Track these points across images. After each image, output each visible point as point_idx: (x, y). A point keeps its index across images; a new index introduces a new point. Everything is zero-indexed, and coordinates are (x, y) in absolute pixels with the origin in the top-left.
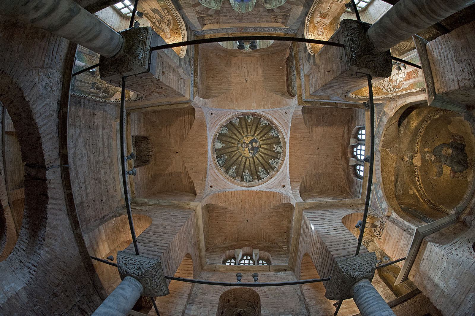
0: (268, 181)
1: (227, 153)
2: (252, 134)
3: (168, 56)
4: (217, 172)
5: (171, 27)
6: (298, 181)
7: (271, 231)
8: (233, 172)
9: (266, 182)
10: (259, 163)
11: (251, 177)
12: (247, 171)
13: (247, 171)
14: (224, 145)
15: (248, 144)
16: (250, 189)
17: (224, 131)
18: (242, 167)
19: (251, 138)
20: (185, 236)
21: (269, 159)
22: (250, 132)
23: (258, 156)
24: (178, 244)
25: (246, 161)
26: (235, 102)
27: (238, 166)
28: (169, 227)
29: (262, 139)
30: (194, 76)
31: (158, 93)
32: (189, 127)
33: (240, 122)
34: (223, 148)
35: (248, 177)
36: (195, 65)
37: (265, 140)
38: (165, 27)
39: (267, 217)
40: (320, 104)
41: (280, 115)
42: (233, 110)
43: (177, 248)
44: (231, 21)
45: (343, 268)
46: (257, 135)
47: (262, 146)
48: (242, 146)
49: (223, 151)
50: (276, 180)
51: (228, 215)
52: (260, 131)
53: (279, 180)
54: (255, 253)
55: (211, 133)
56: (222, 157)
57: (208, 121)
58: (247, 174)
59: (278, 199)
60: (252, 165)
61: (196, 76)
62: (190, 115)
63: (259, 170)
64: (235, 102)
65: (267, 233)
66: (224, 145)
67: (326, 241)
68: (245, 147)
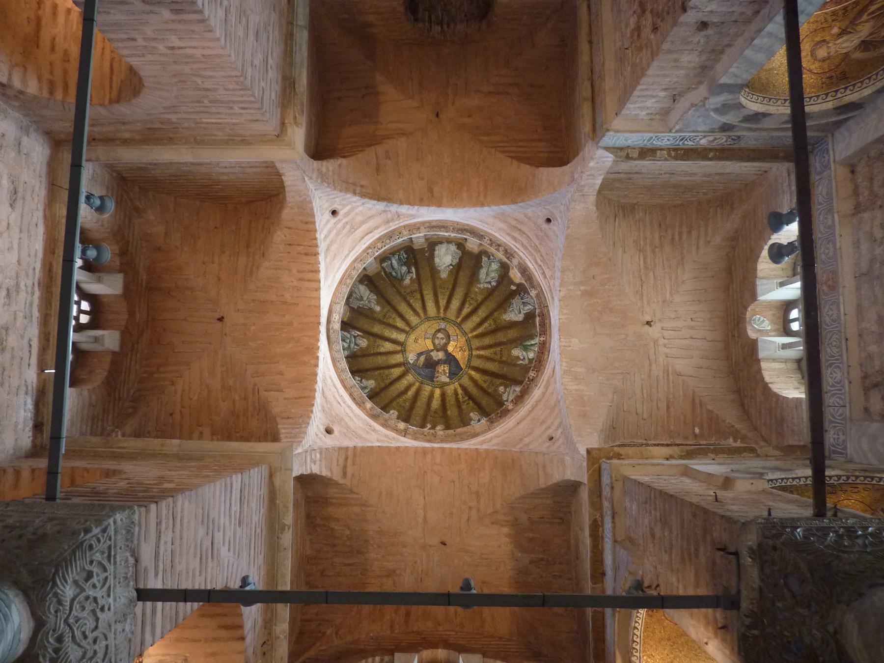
0: (345, 387)
1: (420, 284)
2: (476, 363)
3: (753, 39)
4: (376, 235)
5: (858, 55)
6: (345, 474)
7: (179, 394)
8: (361, 299)
9: (342, 382)
10: (387, 382)
12: (363, 343)
13: (363, 343)
14: (444, 275)
15: (444, 349)
16: (323, 329)
17: (487, 274)
18: (377, 329)
20: (208, 85)
21: (398, 411)
23: (410, 378)
24: (189, 51)
26: (582, 288)
27: (380, 316)
28: (241, 33)
29: (460, 391)
30: (674, 150)
31: (638, 29)
32: (511, 152)
33: (513, 325)
34: (434, 271)
36: (711, 150)
37: (457, 399)
38: (861, 34)
39: (231, 382)
40: (595, 521)
41: (544, 422)
42: (558, 282)
43: (177, 43)
44: (865, 247)
45: (104, 531)
47: (438, 392)
48: (439, 331)
49: (426, 272)
50: (348, 411)
51: (242, 260)
52: (485, 385)
53: (347, 419)
54: (110, 339)
55: (490, 220)
57: (529, 212)
58: (356, 344)
59: (293, 411)
60: (380, 360)
61: (673, 153)
62: (546, 155)
63: (367, 379)
64: (582, 288)
65: (173, 384)
66: (444, 275)
67: (187, 502)
68: (437, 342)
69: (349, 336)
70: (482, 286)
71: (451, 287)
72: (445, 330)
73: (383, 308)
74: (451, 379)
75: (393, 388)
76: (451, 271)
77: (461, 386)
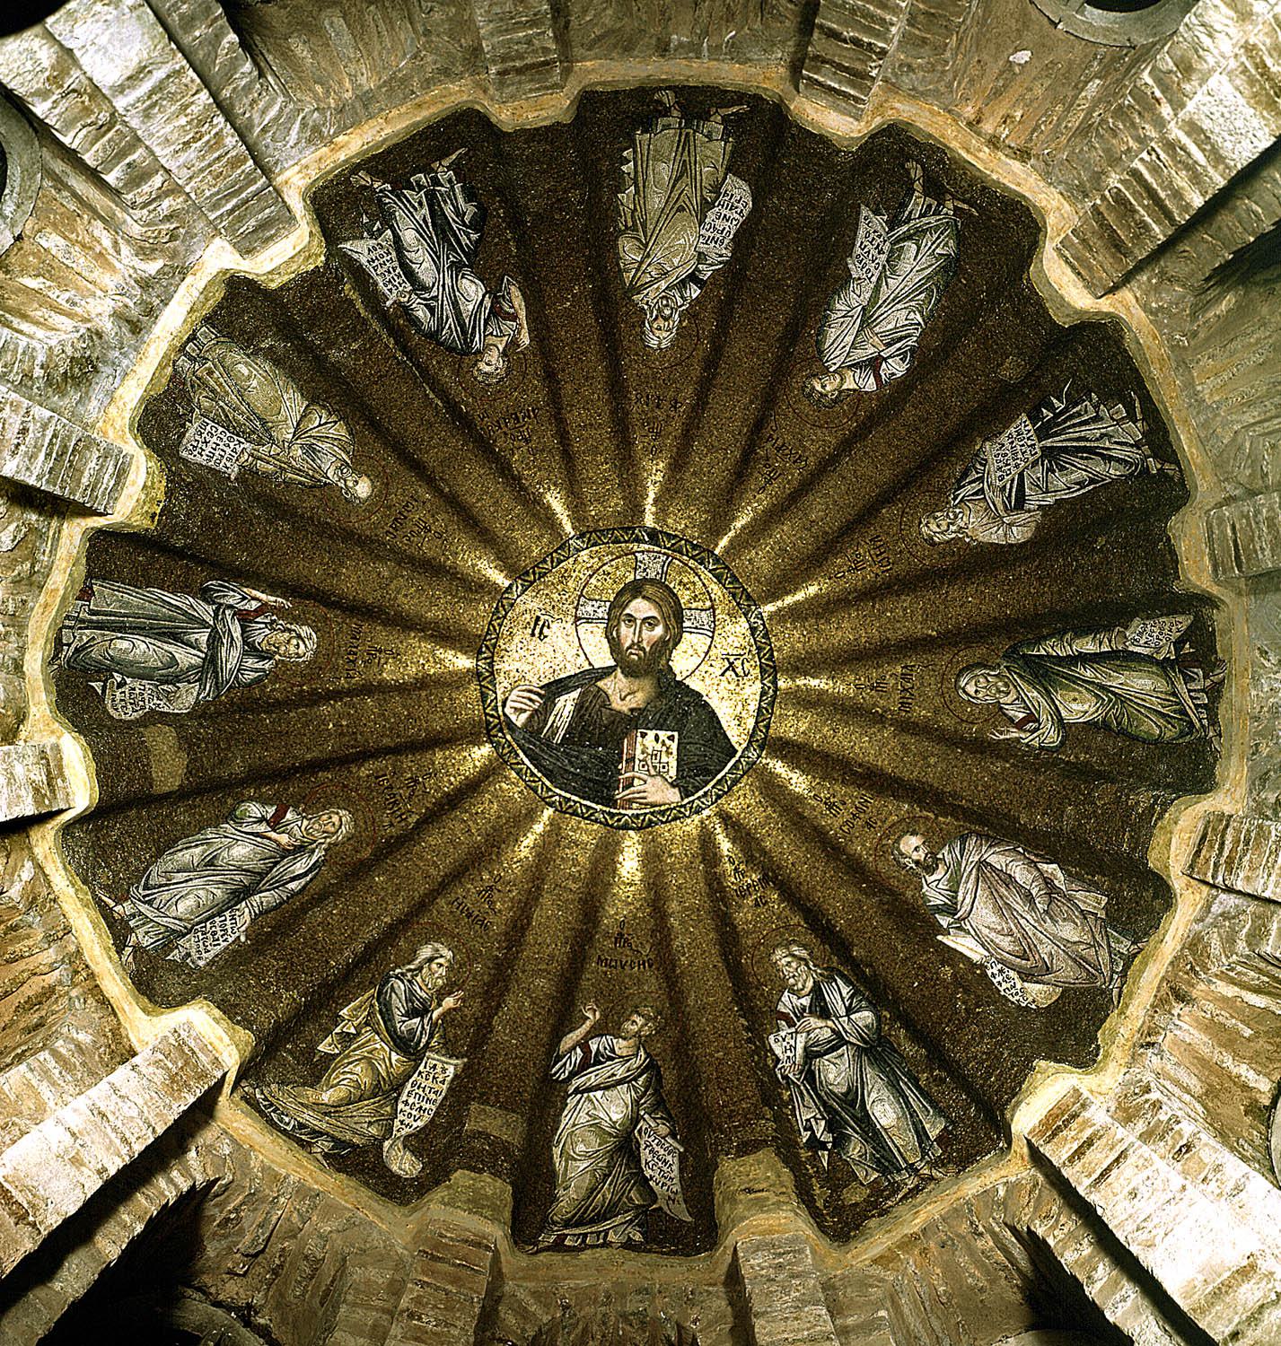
1: (550, 376)
2: (793, 726)
11: (188, 697)
12: (300, 644)
13: (300, 644)
14: (659, 337)
17: (867, 320)
18: (355, 579)
19: (733, 705)
22: (808, 701)
23: (511, 787)
25: (447, 636)
35: (186, 657)
37: (715, 884)
46: (772, 790)
48: (635, 589)
52: (833, 824)
56: (494, 291)
58: (251, 649)
68: (627, 634)
69: (205, 611)
70: (830, 386)
71: (688, 395)
72: (659, 583)
73: (383, 483)
74: (686, 793)
75: (433, 839)
76: (692, 314)
77: (725, 818)
